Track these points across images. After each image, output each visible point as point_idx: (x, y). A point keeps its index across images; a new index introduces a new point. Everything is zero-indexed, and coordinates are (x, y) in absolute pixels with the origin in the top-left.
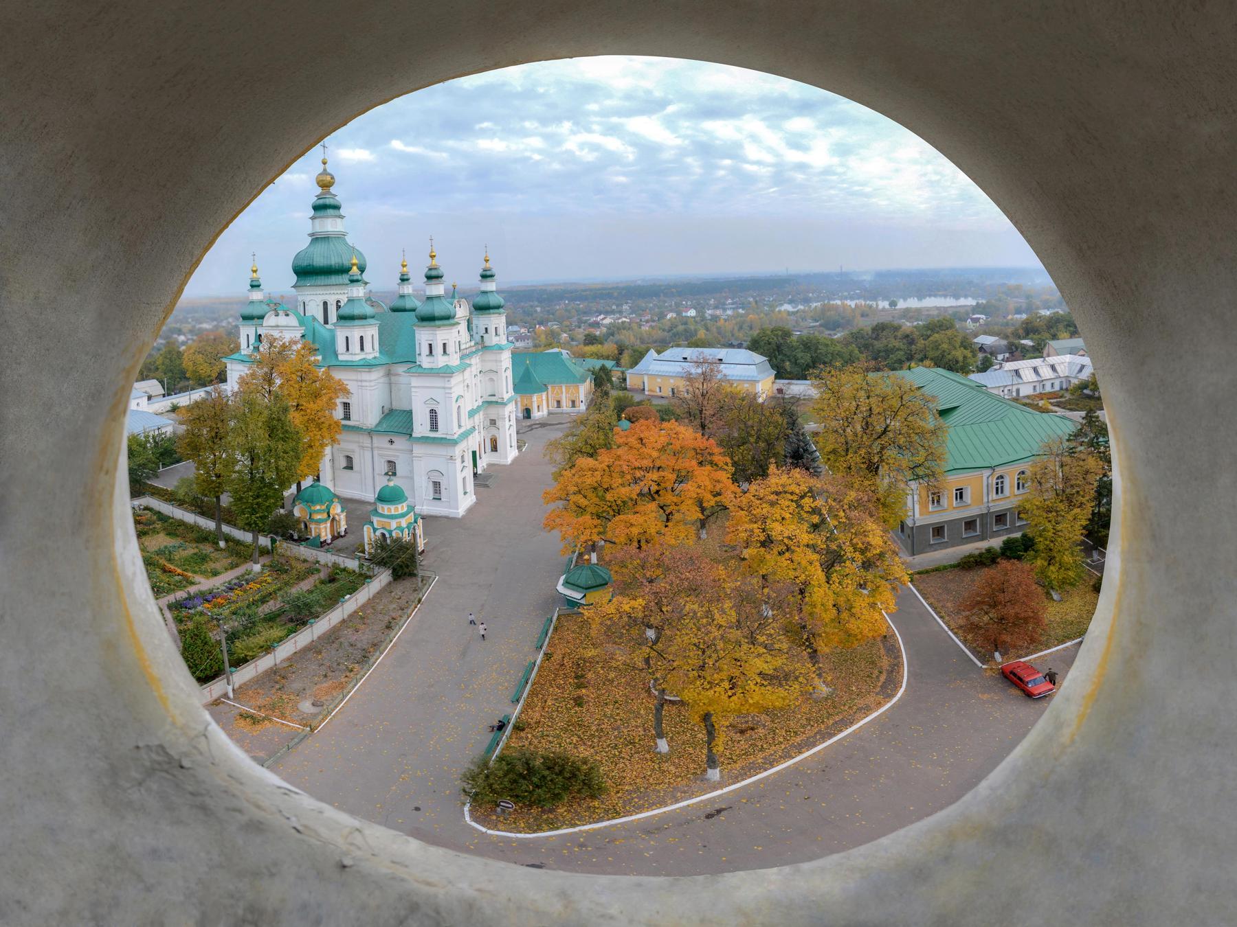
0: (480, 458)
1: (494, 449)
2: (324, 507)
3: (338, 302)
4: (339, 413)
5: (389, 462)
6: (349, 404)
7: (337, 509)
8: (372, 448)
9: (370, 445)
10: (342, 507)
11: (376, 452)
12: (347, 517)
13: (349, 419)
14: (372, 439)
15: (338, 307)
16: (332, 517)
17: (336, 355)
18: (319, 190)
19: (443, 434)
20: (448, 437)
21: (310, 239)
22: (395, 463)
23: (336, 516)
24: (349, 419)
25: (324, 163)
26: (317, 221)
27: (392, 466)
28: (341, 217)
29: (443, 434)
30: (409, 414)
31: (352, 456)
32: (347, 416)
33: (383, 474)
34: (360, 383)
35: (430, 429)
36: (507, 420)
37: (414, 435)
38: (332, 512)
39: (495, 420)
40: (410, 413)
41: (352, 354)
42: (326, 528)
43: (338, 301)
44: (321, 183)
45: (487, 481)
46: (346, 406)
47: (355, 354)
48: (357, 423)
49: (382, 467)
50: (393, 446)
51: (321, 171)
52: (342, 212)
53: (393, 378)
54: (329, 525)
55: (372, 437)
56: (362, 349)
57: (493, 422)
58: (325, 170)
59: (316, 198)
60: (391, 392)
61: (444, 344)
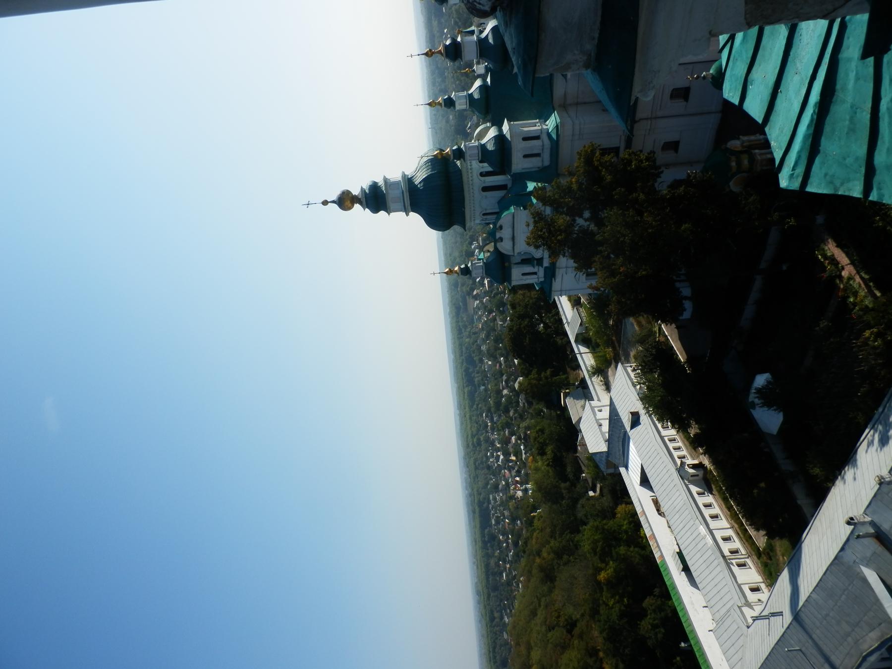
2: (733, 158)
3: (482, 174)
7: (735, 144)
8: (656, 118)
9: (649, 122)
10: (733, 139)
12: (744, 135)
15: (488, 174)
18: (357, 207)
21: (412, 214)
22: (674, 89)
25: (325, 203)
26: (391, 205)
28: (386, 180)
31: (662, 143)
33: (685, 103)
38: (740, 149)
41: (543, 149)
42: (761, 154)
43: (482, 174)
44: (350, 205)
47: (543, 145)
48: (623, 138)
51: (335, 206)
54: (757, 151)
55: (641, 119)
58: (333, 202)
59: (367, 209)
60: (585, 103)
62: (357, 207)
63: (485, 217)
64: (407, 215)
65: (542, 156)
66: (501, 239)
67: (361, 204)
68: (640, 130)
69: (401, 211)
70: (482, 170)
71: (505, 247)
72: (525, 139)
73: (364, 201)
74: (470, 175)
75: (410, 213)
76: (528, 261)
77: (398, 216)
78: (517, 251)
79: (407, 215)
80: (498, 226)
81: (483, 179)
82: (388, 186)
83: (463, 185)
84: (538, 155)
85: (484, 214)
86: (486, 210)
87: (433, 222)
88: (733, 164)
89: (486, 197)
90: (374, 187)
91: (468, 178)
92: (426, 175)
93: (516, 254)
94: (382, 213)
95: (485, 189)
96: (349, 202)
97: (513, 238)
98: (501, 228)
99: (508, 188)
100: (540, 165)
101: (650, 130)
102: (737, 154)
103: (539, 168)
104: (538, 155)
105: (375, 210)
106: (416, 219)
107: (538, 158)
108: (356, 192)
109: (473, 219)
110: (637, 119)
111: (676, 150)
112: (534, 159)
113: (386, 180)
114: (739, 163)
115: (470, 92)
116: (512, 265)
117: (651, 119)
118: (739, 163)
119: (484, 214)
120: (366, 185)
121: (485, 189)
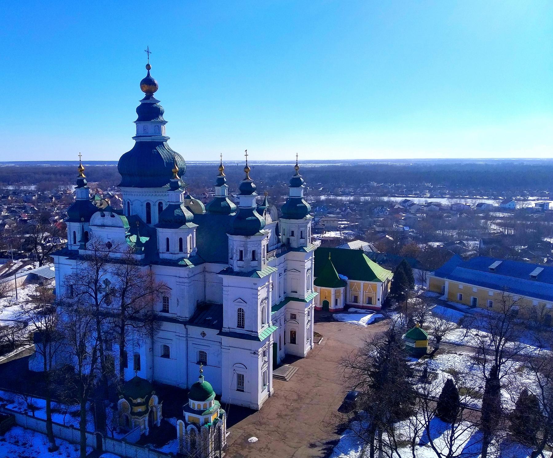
0: (280, 349)
1: (293, 341)
2: (144, 400)
3: (160, 204)
4: (159, 307)
5: (200, 352)
6: (168, 298)
7: (155, 399)
10: (159, 398)
11: (190, 343)
13: (168, 312)
14: (187, 330)
15: (160, 208)
16: (150, 410)
17: (158, 254)
19: (249, 331)
20: (253, 334)
21: (134, 142)
22: (205, 353)
23: (154, 408)
24: (168, 312)
27: (202, 360)
28: (164, 123)
29: (249, 331)
30: (220, 307)
32: (166, 310)
34: (178, 279)
35: (236, 326)
36: (306, 315)
37: (224, 330)
39: (295, 315)
40: (221, 307)
43: (160, 204)
44: (145, 89)
45: (285, 372)
46: (166, 300)
48: (175, 316)
49: (194, 357)
50: (205, 338)
52: (165, 117)
53: (207, 275)
56: (181, 249)
57: (293, 317)
59: (140, 103)
61: (254, 252)
62: (143, 95)
63: (126, 203)
64: (133, 138)
65: (167, 252)
66: (103, 216)
67: (145, 99)
68: (179, 328)
69: (137, 133)
70: (164, 204)
71: (96, 218)
72: (181, 240)
73: (148, 101)
74: (161, 194)
75: (135, 140)
76: (86, 236)
77: (133, 131)
78: (93, 228)
79: (133, 138)
80: (114, 213)
81: (157, 204)
82: (158, 125)
83: (153, 187)
84: (168, 250)
85: (128, 203)
86: (132, 205)
87: (126, 157)
88: (139, 400)
89: (142, 205)
90: (158, 112)
91: (158, 192)
92: (163, 157)
93: (90, 227)
94: (136, 117)
95: (148, 205)
96: (148, 88)
97: (103, 226)
98: (113, 216)
99: (148, 224)
100: (161, 251)
101: (179, 336)
102: (146, 403)
103: (159, 250)
104: (168, 250)
105: (139, 110)
106: (129, 145)
107: (165, 250)
108: (156, 96)
109: (125, 193)
110: (187, 326)
111: (162, 356)
112: (165, 247)
113: (164, 123)
114: (139, 405)
115: (227, 199)
116: (82, 223)
117: (187, 337)
118: (139, 405)
119: (128, 203)
120: (162, 105)
121: (148, 205)
